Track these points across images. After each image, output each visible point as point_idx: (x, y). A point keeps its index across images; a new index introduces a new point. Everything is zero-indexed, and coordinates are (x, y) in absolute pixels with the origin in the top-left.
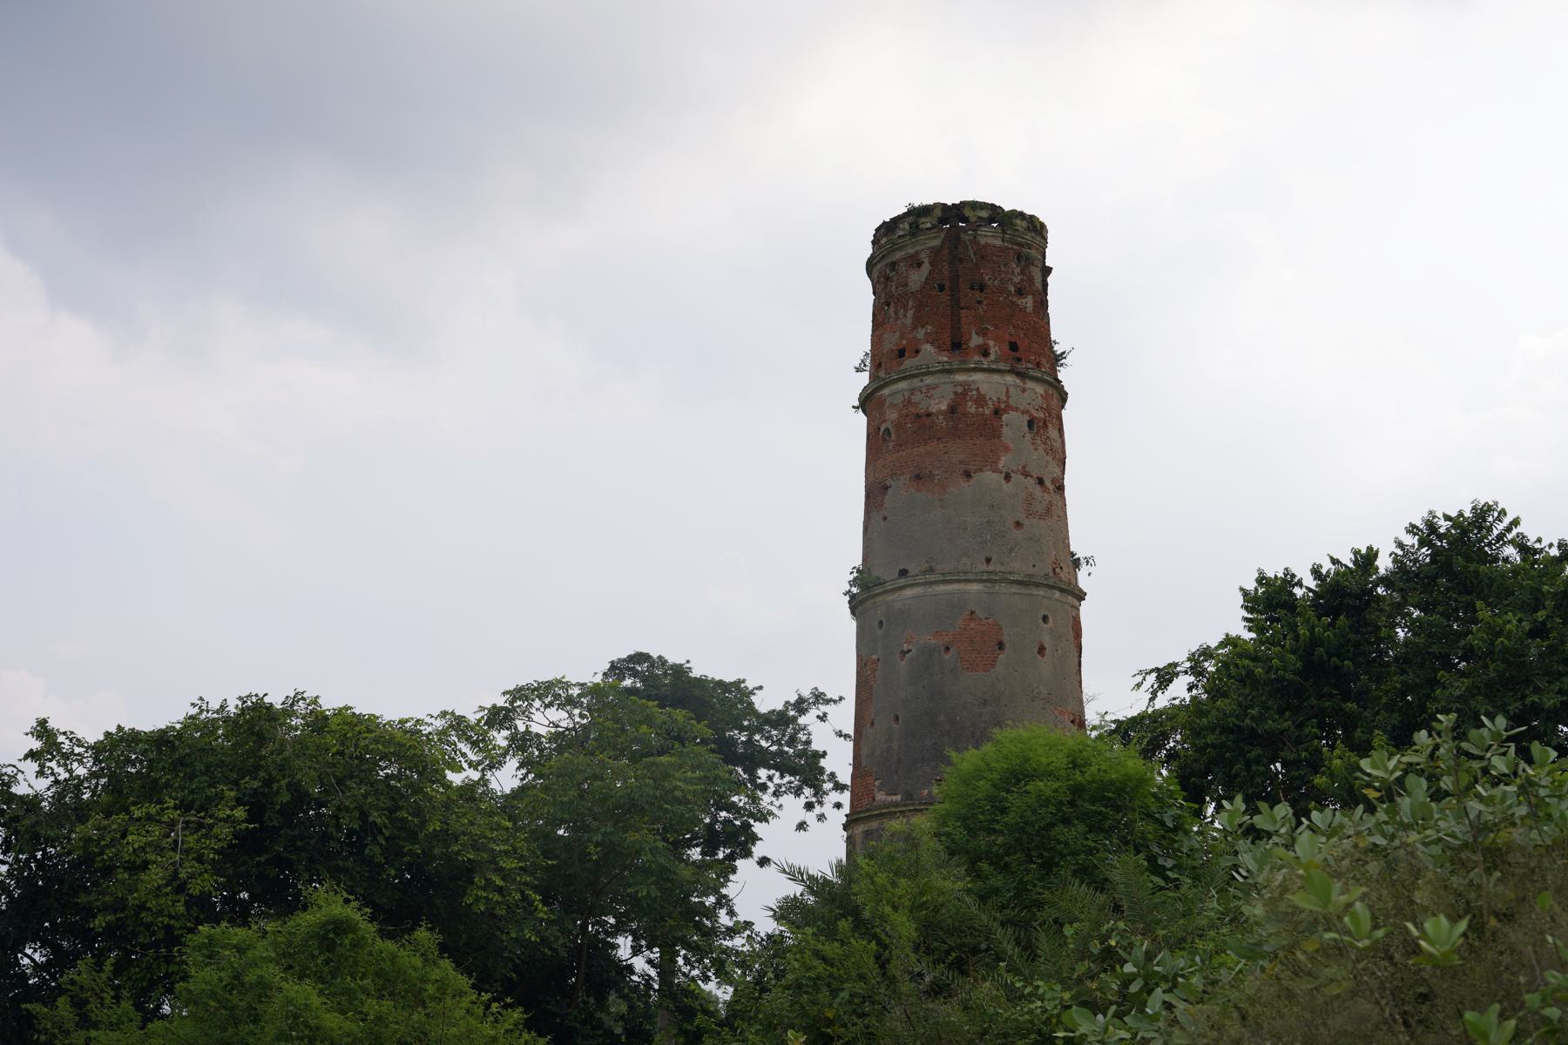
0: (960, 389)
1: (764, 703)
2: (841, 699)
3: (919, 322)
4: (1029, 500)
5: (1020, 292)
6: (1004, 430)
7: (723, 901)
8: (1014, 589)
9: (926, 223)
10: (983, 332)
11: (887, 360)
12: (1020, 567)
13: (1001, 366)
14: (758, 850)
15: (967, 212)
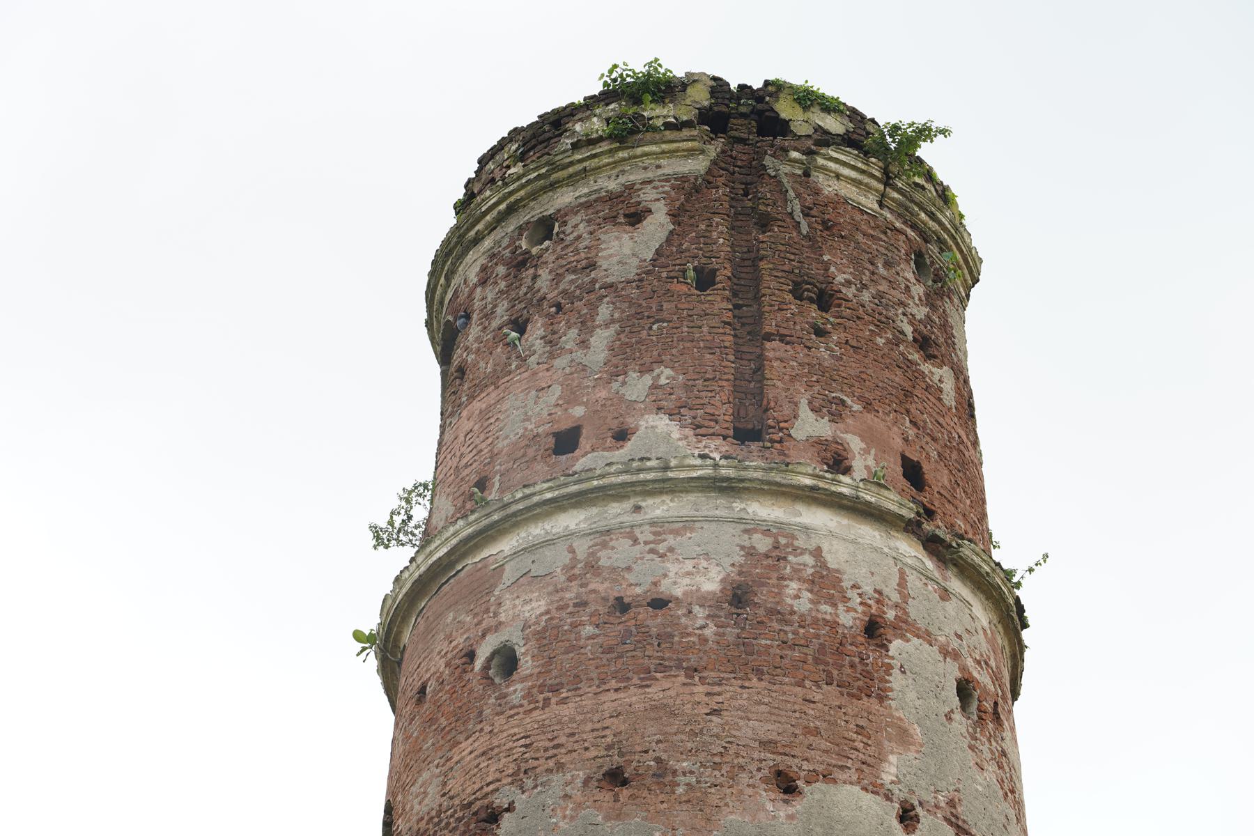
0: (762, 544)
2: (1046, 556)
3: (626, 356)
6: (896, 681)
9: (658, 113)
13: (892, 501)
15: (785, 109)
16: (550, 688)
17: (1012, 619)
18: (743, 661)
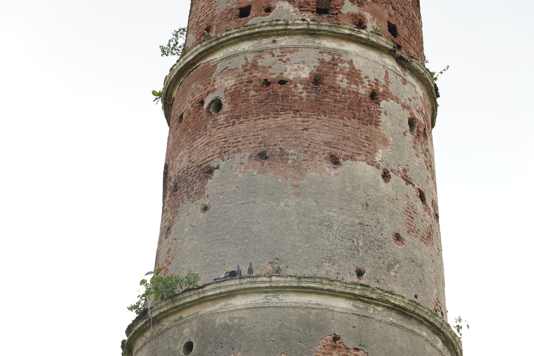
0: (327, 58)
2: (448, 67)
4: (410, 212)
6: (383, 118)
8: (393, 317)
13: (383, 41)
16: (235, 117)
17: (433, 93)
18: (318, 107)
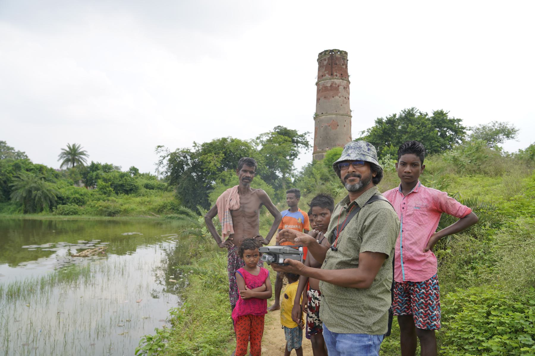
1: (299, 133)
3: (326, 70)
4: (343, 101)
5: (343, 65)
7: (293, 165)
9: (327, 53)
10: (336, 72)
11: (320, 77)
12: (341, 112)
14: (298, 157)
16: (322, 92)
18: (331, 90)
